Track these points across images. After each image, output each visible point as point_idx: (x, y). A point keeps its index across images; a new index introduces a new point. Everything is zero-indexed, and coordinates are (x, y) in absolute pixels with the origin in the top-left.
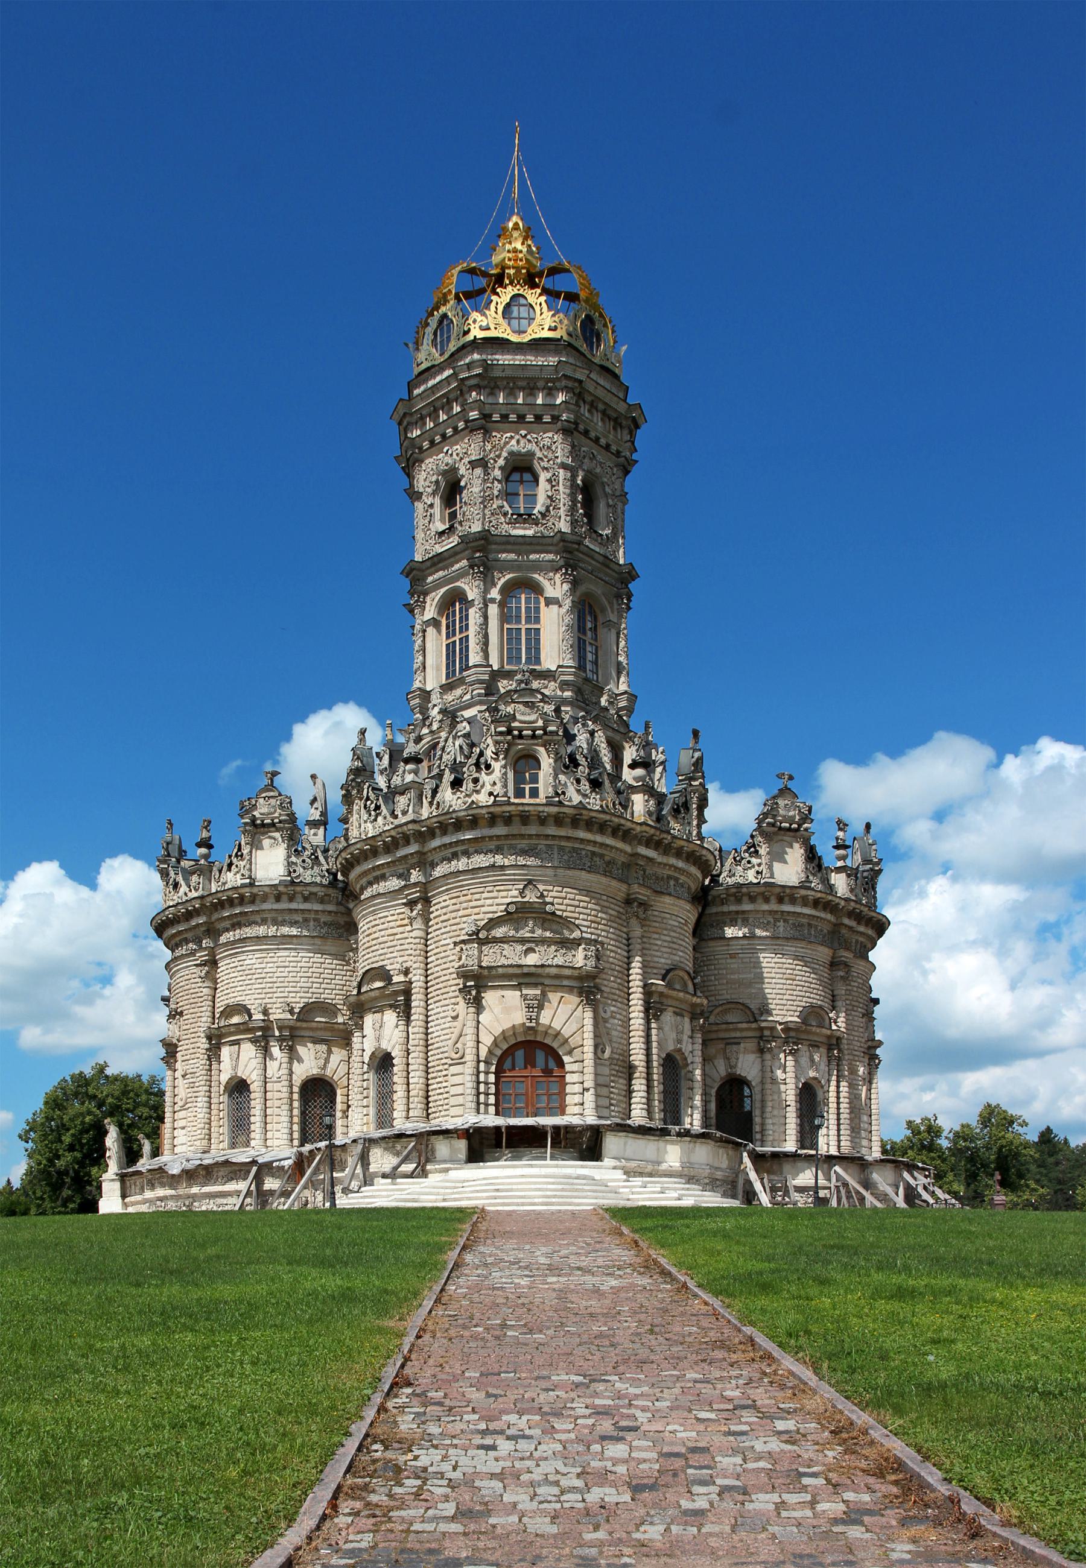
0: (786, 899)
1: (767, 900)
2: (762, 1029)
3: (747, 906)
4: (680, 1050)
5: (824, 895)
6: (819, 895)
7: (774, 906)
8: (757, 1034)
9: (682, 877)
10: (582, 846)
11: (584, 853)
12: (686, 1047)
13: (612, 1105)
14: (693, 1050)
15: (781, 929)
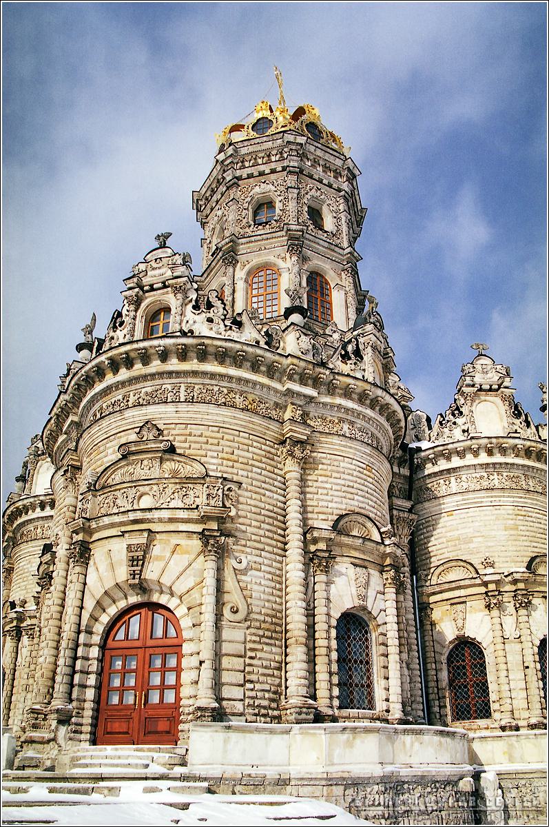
0: (496, 451)
1: (476, 453)
2: (485, 584)
3: (456, 462)
4: (364, 608)
5: (533, 444)
6: (528, 443)
7: (484, 458)
8: (483, 590)
9: (358, 421)
10: (213, 382)
11: (216, 389)
12: (374, 605)
13: (246, 681)
14: (385, 608)
15: (496, 482)
